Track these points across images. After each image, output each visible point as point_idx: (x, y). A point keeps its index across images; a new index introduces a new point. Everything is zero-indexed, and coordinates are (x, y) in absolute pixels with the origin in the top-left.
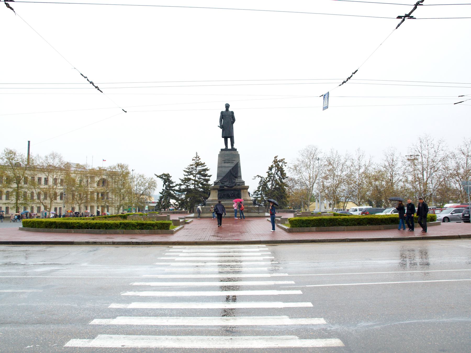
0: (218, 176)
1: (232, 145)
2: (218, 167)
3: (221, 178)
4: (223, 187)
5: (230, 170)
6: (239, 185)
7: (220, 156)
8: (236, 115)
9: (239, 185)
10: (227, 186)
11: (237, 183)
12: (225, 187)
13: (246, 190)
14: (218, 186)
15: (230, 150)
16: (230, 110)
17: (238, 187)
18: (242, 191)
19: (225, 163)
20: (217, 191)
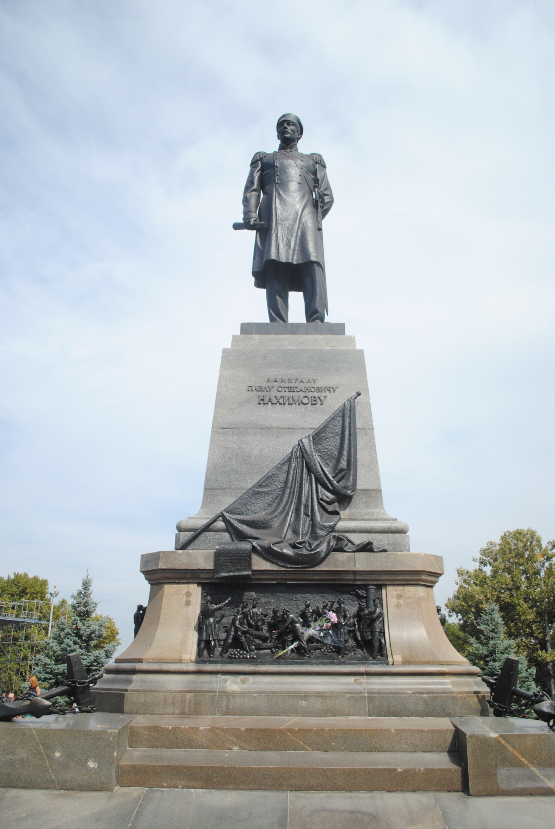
0: (211, 490)
1: (314, 313)
2: (220, 429)
3: (228, 501)
4: (243, 559)
5: (301, 447)
6: (367, 548)
7: (230, 359)
8: (335, 177)
9: (367, 548)
10: (269, 554)
11: (352, 536)
12: (260, 564)
13: (421, 591)
14: (201, 558)
15: (296, 329)
16: (304, 146)
17: (362, 563)
18: (391, 595)
19: (262, 402)
20: (196, 591)
